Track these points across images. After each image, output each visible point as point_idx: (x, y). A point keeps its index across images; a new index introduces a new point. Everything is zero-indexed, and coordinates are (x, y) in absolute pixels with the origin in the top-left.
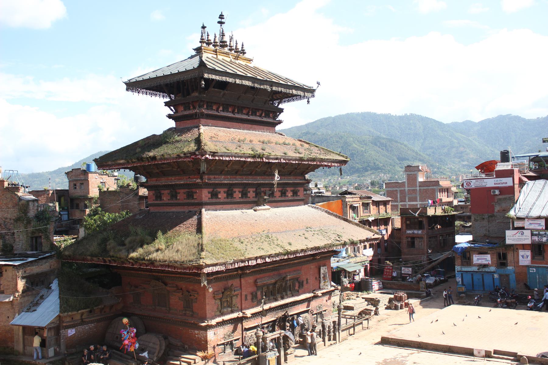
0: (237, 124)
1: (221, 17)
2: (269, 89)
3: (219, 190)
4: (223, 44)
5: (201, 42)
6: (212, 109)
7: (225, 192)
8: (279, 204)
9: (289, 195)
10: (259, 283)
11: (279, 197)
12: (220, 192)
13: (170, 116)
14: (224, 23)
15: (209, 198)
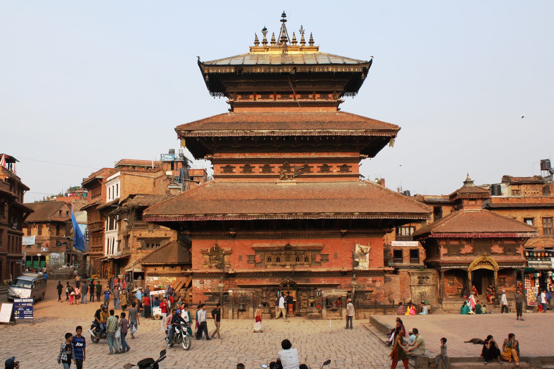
0: (281, 108)
1: (284, 15)
2: (293, 72)
3: (234, 165)
4: (284, 39)
5: (255, 43)
6: (248, 98)
7: (241, 167)
8: (317, 180)
9: (335, 171)
10: (255, 245)
11: (318, 172)
12: (235, 167)
13: (229, 110)
14: (286, 21)
15: (221, 172)
